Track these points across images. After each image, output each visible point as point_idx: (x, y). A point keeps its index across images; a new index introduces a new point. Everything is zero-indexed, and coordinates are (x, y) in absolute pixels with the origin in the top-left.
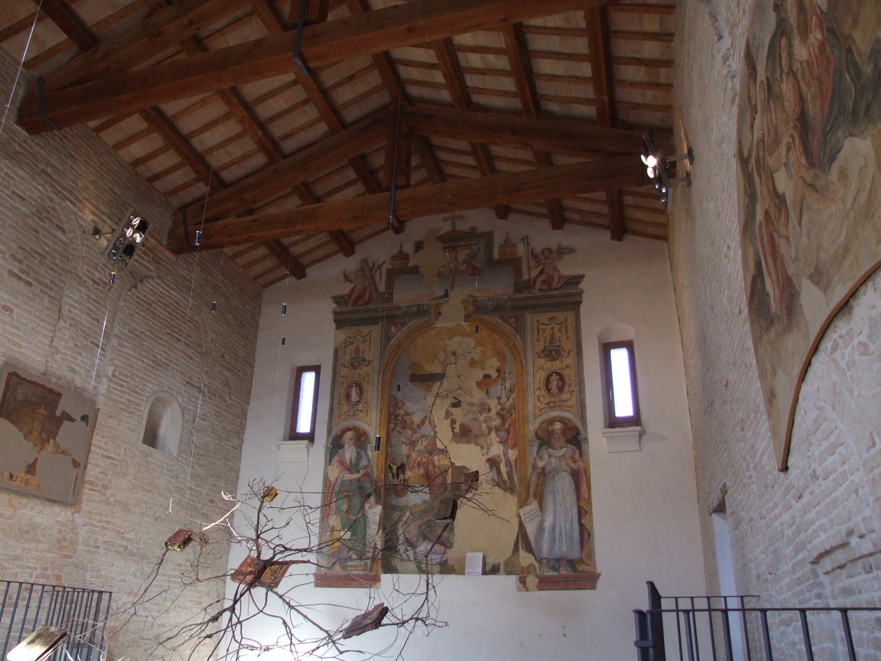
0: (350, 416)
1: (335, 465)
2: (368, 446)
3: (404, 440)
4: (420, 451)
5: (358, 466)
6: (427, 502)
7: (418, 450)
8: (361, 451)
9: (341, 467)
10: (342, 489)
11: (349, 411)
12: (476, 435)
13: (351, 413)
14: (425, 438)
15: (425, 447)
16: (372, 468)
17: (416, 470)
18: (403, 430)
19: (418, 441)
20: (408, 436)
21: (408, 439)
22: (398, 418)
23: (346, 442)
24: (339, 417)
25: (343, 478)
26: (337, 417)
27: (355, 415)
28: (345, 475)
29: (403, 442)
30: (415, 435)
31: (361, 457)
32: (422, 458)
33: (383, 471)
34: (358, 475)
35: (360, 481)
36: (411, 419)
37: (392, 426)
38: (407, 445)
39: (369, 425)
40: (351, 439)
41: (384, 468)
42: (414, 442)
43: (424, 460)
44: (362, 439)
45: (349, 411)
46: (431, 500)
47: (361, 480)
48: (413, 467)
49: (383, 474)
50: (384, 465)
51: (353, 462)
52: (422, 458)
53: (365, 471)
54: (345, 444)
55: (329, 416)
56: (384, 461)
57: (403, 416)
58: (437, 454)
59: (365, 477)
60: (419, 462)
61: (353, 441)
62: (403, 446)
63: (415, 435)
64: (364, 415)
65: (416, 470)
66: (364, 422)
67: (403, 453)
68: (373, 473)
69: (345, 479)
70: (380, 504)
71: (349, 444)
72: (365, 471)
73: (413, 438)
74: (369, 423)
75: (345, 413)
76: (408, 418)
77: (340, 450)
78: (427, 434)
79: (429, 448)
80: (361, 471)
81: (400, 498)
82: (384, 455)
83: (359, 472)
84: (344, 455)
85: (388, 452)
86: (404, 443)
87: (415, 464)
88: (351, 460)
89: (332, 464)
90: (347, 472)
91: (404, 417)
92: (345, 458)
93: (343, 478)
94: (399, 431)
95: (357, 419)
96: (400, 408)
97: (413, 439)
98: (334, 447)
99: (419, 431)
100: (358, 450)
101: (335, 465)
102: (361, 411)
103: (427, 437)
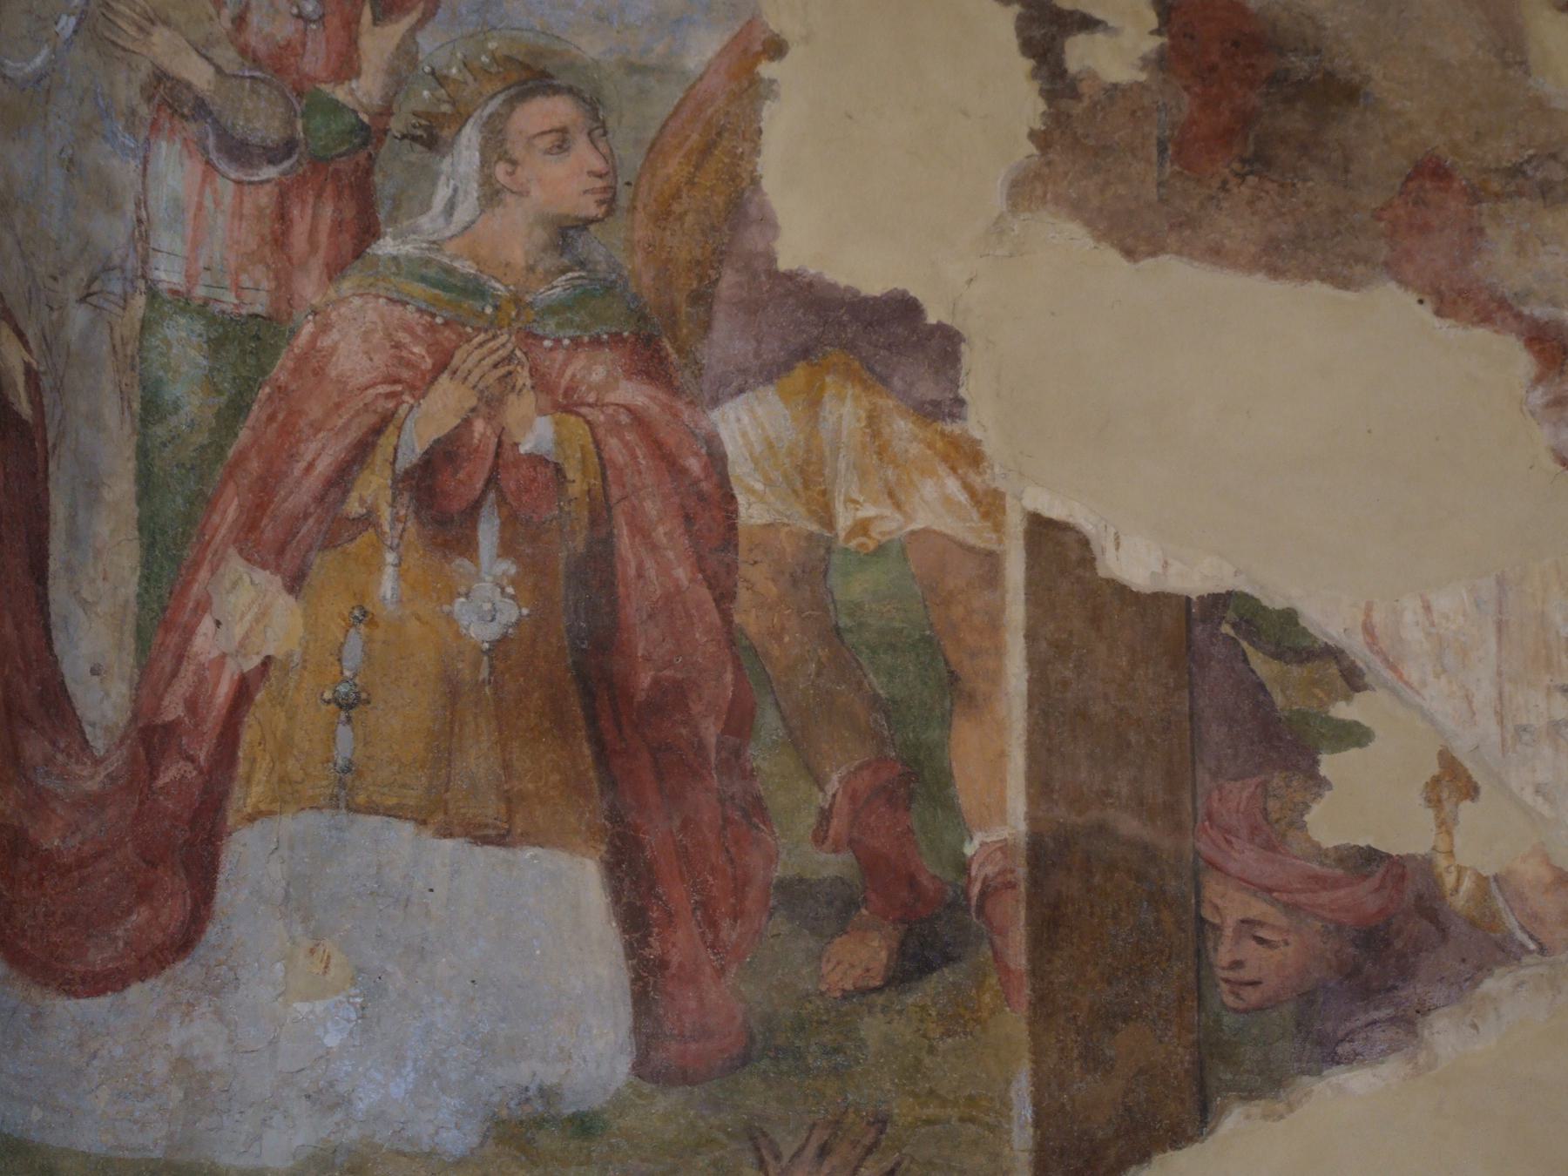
3: (198, 74)
4: (474, 289)
6: (584, 1125)
7: (418, 270)
12: (1432, 171)
17: (387, 585)
32: (491, 404)
38: (239, 151)
52: (491, 404)
58: (771, 373)
65: (387, 585)
67: (168, 274)
73: (347, 66)
78: (591, 47)
86: (201, 108)
103: (592, 105)
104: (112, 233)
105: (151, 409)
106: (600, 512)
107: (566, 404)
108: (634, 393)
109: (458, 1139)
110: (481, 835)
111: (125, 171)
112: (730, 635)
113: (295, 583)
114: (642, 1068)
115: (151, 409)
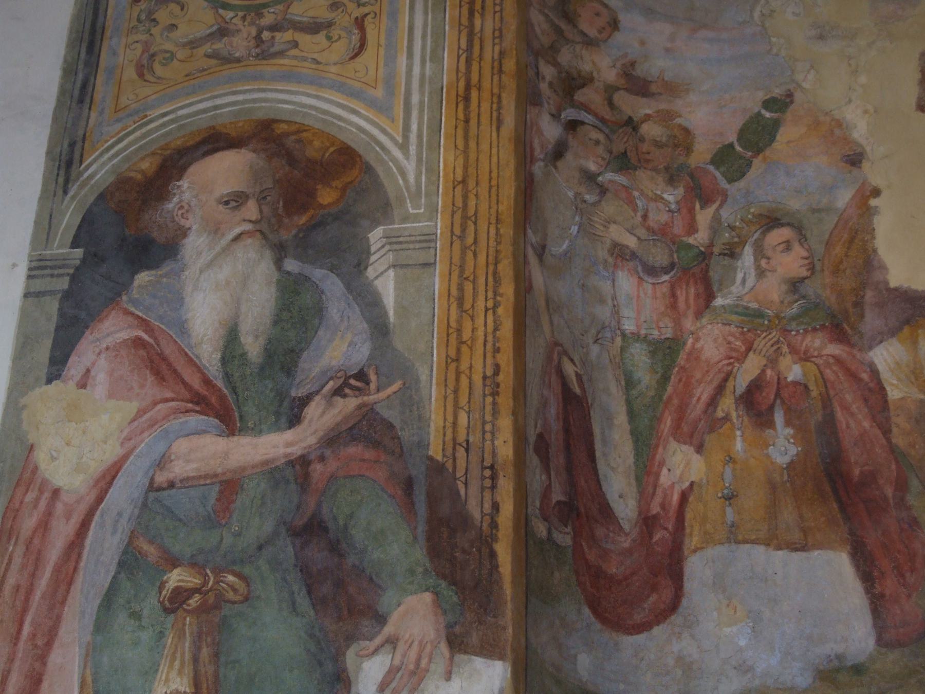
0: (227, 60)
1: (101, 377)
2: (376, 236)
3: (631, 242)
4: (759, 314)
5: (289, 370)
6: (858, 669)
7: (734, 309)
8: (318, 274)
9: (151, 389)
10: (151, 550)
11: (223, 32)
13: (240, 44)
14: (785, 233)
15: (795, 285)
16: (410, 386)
17: (739, 445)
18: (620, 179)
19: (732, 253)
20: (658, 217)
21: (662, 233)
22: (579, 96)
23: (193, 222)
24: (143, 70)
25: (162, 463)
26: (130, 73)
27: (264, 56)
28: (182, 446)
29: (620, 253)
30: (704, 217)
31: (319, 310)
32: (773, 362)
33: (506, 401)
34: (289, 435)
35: (304, 480)
36: (666, 117)
37: (551, 131)
38: (652, 271)
39: (372, 104)
40: (236, 200)
41: (506, 379)
42: (704, 256)
43: (794, 372)
44: (326, 196)
45: (223, 32)
46: (893, 660)
47: (317, 469)
48: (714, 425)
49: (506, 423)
50: (506, 359)
51: (253, 347)
52: (773, 362)
53: (348, 405)
54: (184, 232)
55: (69, 71)
56: (508, 326)
57: (610, 90)
58: (893, 332)
59: (353, 450)
60: (755, 387)
61: (251, 210)
62: (626, 282)
63: (704, 217)
64: (341, 48)
65: (739, 445)
66: (340, 88)
67: (629, 326)
68: (422, 421)
69: (179, 469)
70: (489, 650)
71: (216, 230)
72: (348, 405)
73: (692, 228)
74: (379, 93)
75: (193, 44)
76: (641, 108)
77: (143, 277)
78: (795, 204)
79: (816, 288)
80: (313, 410)
81: (629, 641)
82: (508, 289)
83: (294, 420)
84: (178, 300)
85: (530, 289)
86: (634, 255)
87: (727, 404)
88: (232, 336)
89: (75, 367)
90: (195, 420)
91: (620, 98)
92: (183, 327)
93: (162, 463)
94: (590, 178)
95: (288, 76)
96: (590, 43)
97: (701, 238)
98: (93, 259)
99: (735, 190)
100: (291, 265)
101: (101, 377)
102: (314, 28)
104: (604, 313)
105: (629, 383)
106: (826, 401)
107: (805, 358)
108: (834, 349)
109: (803, 680)
110: (795, 547)
111: (606, 287)
112: (892, 449)
113: (699, 449)
114: (879, 641)
115: (629, 383)
